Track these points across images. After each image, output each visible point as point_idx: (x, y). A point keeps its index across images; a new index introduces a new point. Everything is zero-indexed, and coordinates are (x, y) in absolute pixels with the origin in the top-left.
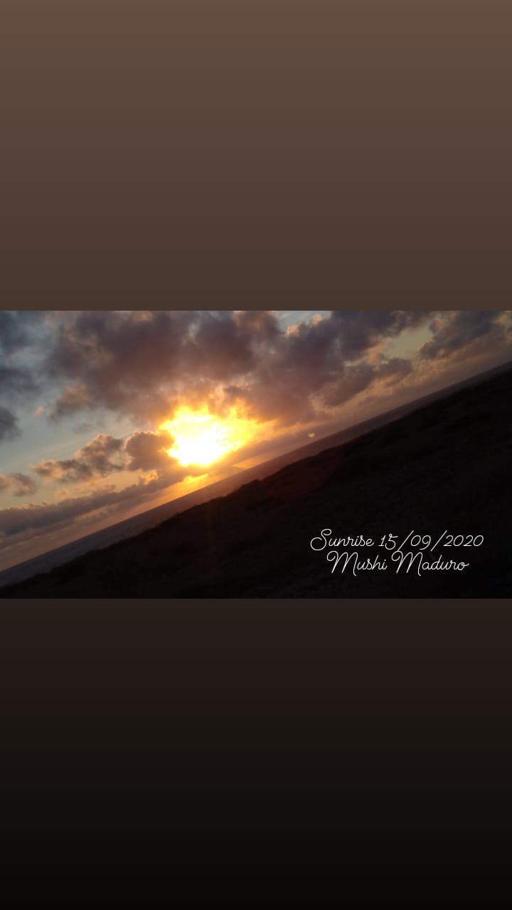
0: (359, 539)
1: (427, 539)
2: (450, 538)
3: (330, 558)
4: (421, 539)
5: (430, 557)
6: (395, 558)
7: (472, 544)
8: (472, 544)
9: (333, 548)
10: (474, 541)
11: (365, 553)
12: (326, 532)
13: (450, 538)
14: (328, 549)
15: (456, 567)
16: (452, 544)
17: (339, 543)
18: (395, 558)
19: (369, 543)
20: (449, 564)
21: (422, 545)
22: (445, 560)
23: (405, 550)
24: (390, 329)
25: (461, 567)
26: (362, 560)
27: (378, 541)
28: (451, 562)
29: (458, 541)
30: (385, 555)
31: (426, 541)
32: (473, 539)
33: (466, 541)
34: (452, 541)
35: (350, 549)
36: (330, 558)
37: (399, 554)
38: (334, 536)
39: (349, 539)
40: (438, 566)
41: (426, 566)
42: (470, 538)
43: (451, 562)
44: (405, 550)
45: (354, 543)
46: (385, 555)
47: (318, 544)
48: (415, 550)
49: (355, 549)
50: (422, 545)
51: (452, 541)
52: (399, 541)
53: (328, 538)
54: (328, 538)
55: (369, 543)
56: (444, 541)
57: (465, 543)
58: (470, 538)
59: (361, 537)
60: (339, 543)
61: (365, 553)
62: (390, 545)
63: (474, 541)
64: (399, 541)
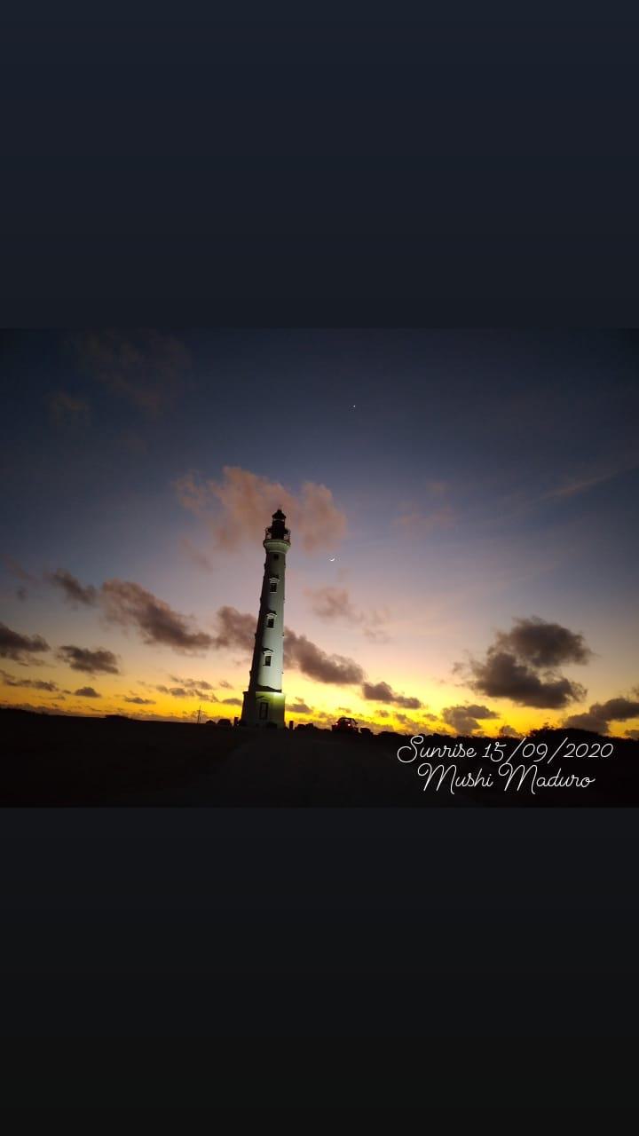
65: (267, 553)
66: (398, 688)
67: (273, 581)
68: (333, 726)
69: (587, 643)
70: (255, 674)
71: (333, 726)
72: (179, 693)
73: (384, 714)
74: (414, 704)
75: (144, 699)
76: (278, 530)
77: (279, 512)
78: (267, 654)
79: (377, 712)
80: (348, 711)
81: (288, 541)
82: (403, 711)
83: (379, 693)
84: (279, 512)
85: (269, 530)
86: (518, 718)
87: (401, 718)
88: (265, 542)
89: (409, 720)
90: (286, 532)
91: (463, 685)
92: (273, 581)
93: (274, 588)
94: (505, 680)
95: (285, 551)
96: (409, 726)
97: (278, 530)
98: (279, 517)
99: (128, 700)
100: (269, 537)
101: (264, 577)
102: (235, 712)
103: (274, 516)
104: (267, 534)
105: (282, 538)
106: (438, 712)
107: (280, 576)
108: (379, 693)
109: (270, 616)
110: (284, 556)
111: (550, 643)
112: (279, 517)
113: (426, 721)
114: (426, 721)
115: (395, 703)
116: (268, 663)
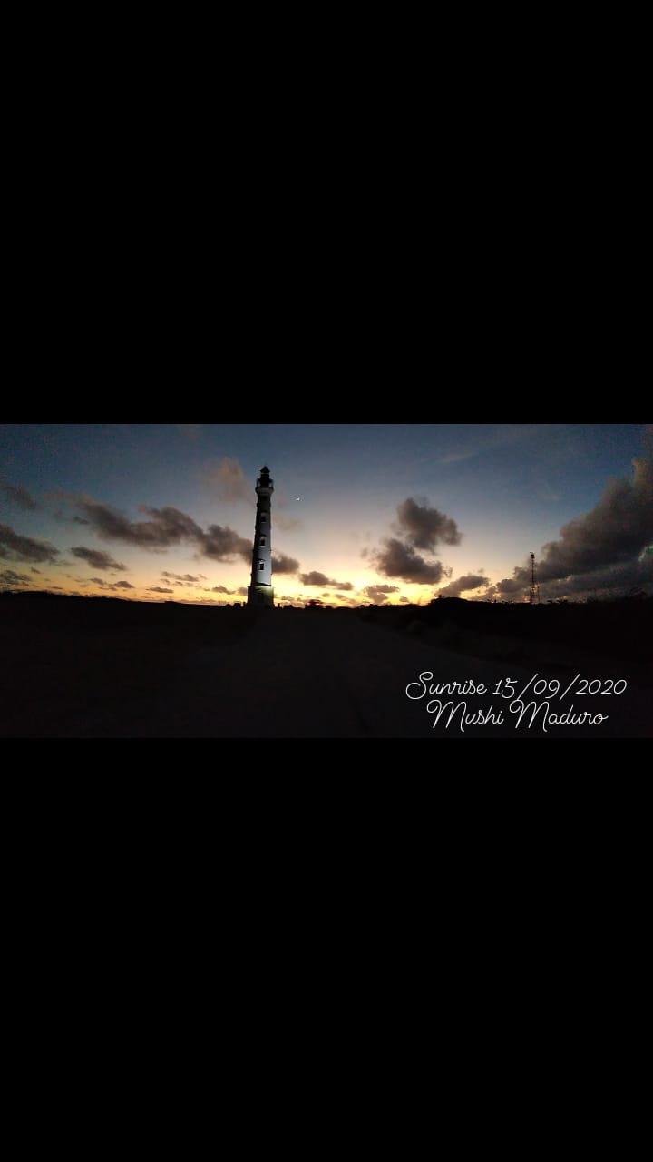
0: (468, 684)
1: (554, 685)
2: (584, 684)
4: (547, 685)
5: (558, 707)
6: (514, 709)
7: (611, 690)
8: (611, 690)
9: (435, 696)
10: (614, 687)
11: (475, 703)
12: (425, 676)
13: (584, 684)
14: (429, 697)
16: (586, 690)
17: (442, 690)
18: (514, 709)
19: (480, 690)
21: (548, 693)
22: (578, 712)
23: (526, 699)
25: (597, 720)
26: (472, 711)
27: (491, 688)
28: (586, 714)
29: (595, 687)
30: (500, 706)
31: (553, 687)
32: (614, 685)
33: (604, 688)
34: (587, 687)
35: (457, 698)
37: (518, 704)
39: (455, 684)
40: (569, 719)
41: (553, 719)
42: (609, 684)
43: (586, 714)
44: (526, 699)
45: (461, 690)
47: (416, 691)
48: (539, 699)
49: (463, 697)
50: (548, 693)
51: (587, 687)
52: (519, 688)
53: (428, 684)
54: (428, 684)
55: (480, 690)
56: (577, 687)
57: (602, 690)
58: (609, 684)
59: (471, 682)
60: (442, 690)
61: (475, 703)
62: (508, 692)
63: (614, 687)
64: (519, 688)
68: (306, 605)
71: (306, 605)
86: (419, 593)
102: (244, 599)
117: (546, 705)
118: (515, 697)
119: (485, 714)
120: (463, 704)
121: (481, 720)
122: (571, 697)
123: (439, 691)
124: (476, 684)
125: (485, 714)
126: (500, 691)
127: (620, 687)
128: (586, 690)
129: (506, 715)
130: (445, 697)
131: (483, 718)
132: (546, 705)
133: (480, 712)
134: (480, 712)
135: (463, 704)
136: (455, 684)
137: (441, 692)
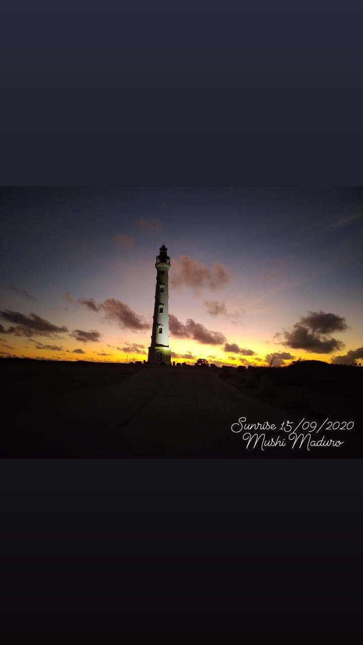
0: (266, 424)
1: (314, 425)
2: (330, 424)
3: (245, 438)
4: (310, 425)
5: (316, 437)
6: (291, 438)
7: (345, 428)
8: (345, 428)
9: (247, 431)
10: (347, 426)
11: (270, 435)
12: (242, 420)
13: (330, 424)
14: (244, 431)
15: (334, 444)
16: (331, 428)
17: (251, 427)
18: (291, 438)
19: (272, 427)
20: (330, 442)
21: (310, 429)
22: (327, 439)
23: (298, 432)
24: (221, 336)
25: (338, 444)
26: (268, 439)
27: (279, 426)
28: (331, 441)
29: (336, 426)
30: (284, 436)
31: (313, 426)
32: (347, 425)
33: (341, 426)
34: (332, 426)
35: (259, 432)
36: (245, 438)
37: (294, 435)
38: (247, 423)
39: (259, 424)
40: (321, 443)
41: (313, 444)
42: (344, 424)
43: (331, 441)
44: (298, 432)
45: (262, 427)
46: (284, 436)
47: (237, 428)
48: (305, 433)
49: (263, 431)
50: (310, 429)
51: (332, 426)
52: (294, 426)
53: (243, 424)
54: (243, 424)
55: (272, 427)
56: (326, 426)
57: (340, 427)
58: (344, 424)
59: (267, 423)
60: (251, 427)
61: (270, 435)
62: (288, 428)
63: (347, 426)
64: (294, 426)
65: (158, 270)
66: (242, 346)
67: (161, 287)
69: (348, 322)
70: (154, 338)
72: (126, 350)
73: (233, 359)
74: (250, 353)
75: (107, 354)
76: (163, 257)
77: (164, 246)
78: (160, 327)
79: (229, 357)
80: (214, 357)
81: (169, 264)
82: (244, 357)
83: (232, 348)
84: (164, 246)
85: (159, 257)
87: (242, 360)
88: (156, 264)
89: (247, 361)
90: (168, 258)
91: (279, 344)
92: (161, 287)
93: (162, 291)
94: (300, 340)
95: (168, 270)
96: (246, 364)
97: (163, 257)
98: (163, 249)
99: (99, 355)
100: (159, 261)
101: (157, 285)
103: (160, 249)
104: (157, 260)
105: (166, 262)
106: (263, 357)
107: (165, 284)
108: (232, 348)
109: (160, 307)
110: (167, 272)
111: (330, 322)
112: (163, 249)
113: (256, 361)
114: (256, 361)
115: (241, 350)
116: (161, 332)
117: (309, 435)
118: (292, 431)
119: (275, 441)
120: (263, 435)
121: (273, 444)
122: (323, 431)
123: (250, 427)
124: (270, 424)
125: (275, 441)
126: (283, 428)
127: (350, 426)
128: (331, 428)
129: (287, 441)
130: (253, 432)
131: (274, 443)
132: (309, 435)
133: (272, 439)
134: (272, 439)
135: (263, 435)
136: (259, 424)
137: (251, 429)
